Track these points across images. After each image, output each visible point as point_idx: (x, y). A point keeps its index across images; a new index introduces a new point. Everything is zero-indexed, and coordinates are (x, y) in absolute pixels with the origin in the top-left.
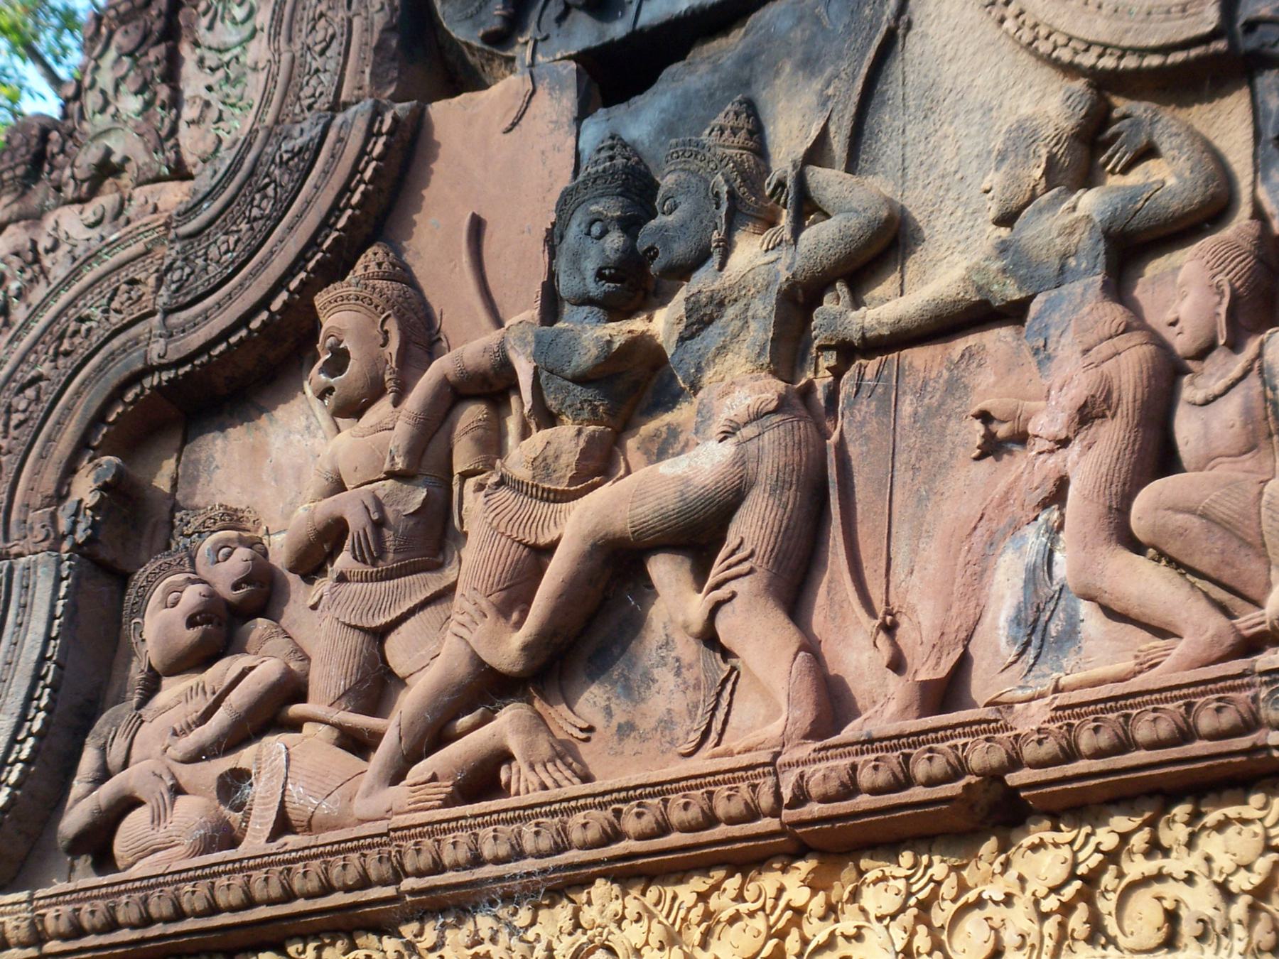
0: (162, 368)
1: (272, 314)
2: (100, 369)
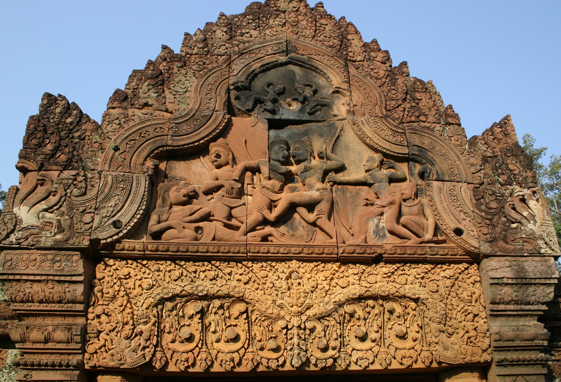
0: (170, 146)
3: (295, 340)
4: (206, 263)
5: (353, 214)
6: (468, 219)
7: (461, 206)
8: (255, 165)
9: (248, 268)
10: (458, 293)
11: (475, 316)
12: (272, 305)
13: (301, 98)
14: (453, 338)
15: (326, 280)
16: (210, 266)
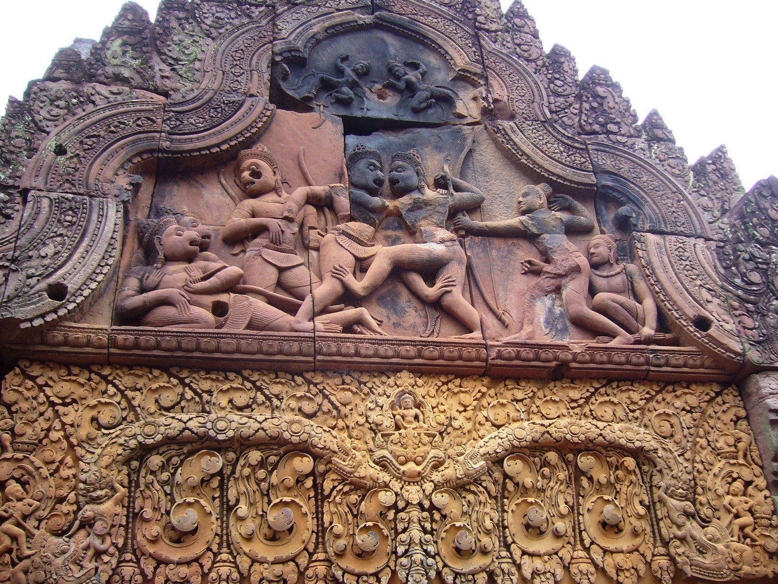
1: (221, 150)
2: (134, 142)
3: (416, 533)
4: (232, 375)
5: (506, 290)
6: (716, 301)
7: (700, 278)
8: (323, 194)
9: (315, 385)
10: (710, 439)
11: (747, 484)
12: (365, 459)
13: (402, 85)
14: (710, 529)
15: (465, 411)
16: (240, 380)
